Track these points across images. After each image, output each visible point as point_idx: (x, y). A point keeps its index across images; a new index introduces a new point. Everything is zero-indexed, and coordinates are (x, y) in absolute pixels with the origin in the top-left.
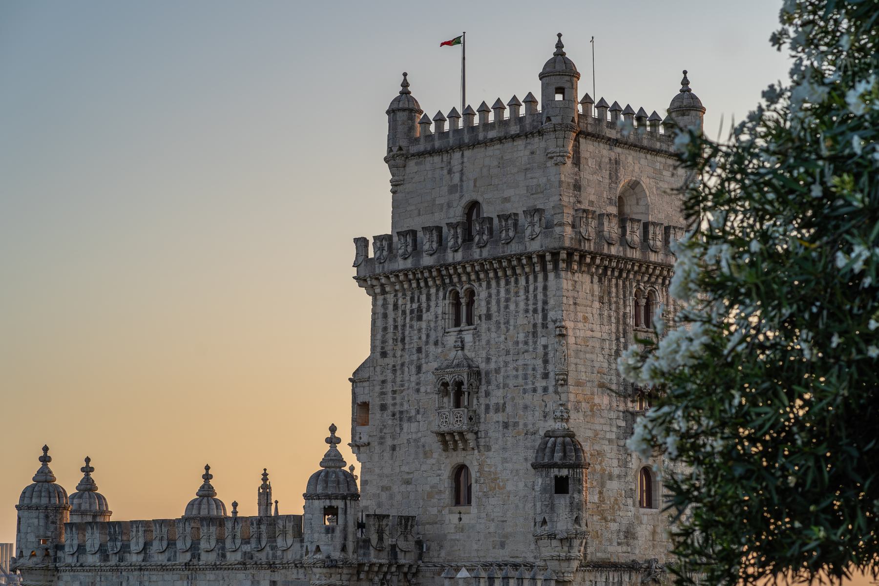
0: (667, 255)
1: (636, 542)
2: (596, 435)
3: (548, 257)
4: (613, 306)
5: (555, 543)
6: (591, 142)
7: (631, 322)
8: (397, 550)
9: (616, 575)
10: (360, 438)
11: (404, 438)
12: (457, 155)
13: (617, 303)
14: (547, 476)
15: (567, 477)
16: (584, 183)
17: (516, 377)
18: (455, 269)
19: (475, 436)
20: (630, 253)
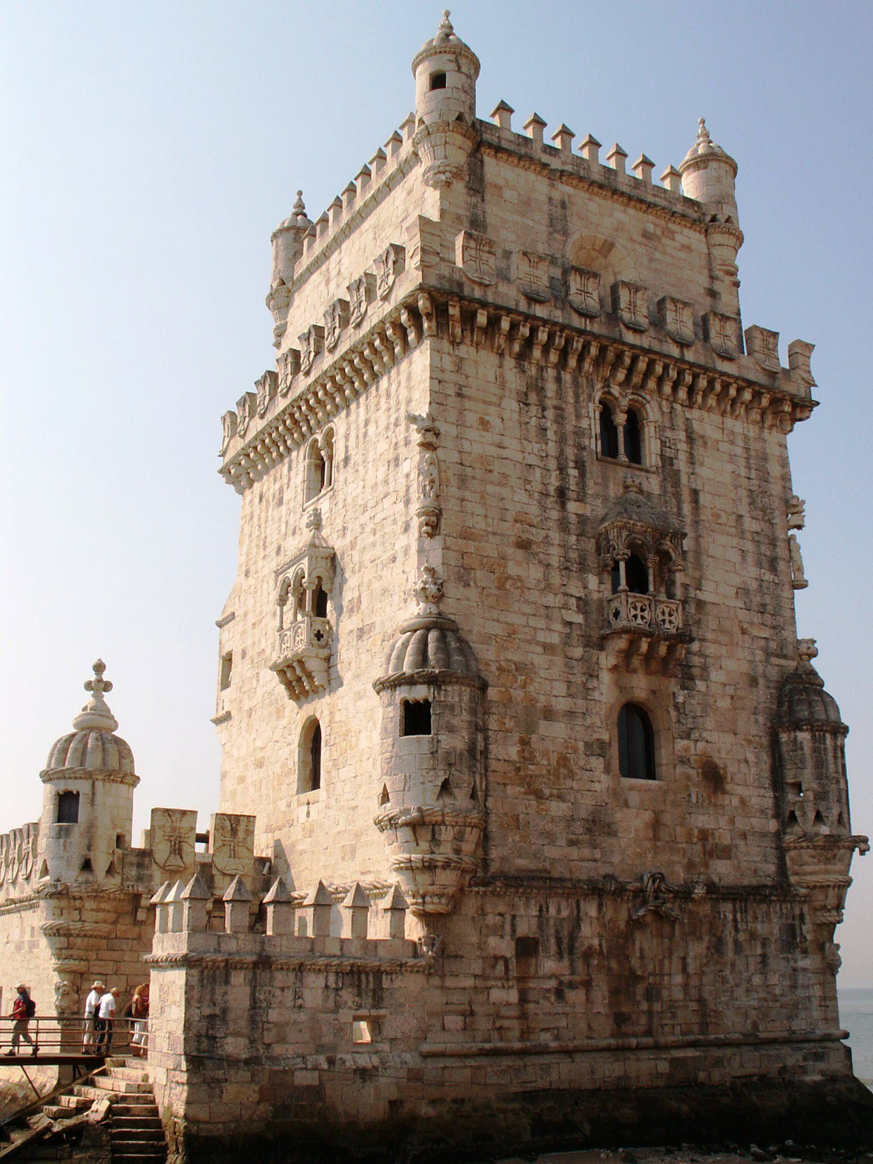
0: (661, 341)
1: (613, 840)
2: (514, 633)
3: (404, 318)
4: (550, 413)
5: (404, 834)
6: (506, 166)
7: (594, 445)
8: (214, 872)
9: (564, 904)
10: (223, 709)
11: (260, 691)
12: (335, 257)
14: (389, 705)
15: (426, 701)
16: (491, 220)
17: (373, 545)
18: (307, 401)
19: (324, 665)
20: (577, 322)
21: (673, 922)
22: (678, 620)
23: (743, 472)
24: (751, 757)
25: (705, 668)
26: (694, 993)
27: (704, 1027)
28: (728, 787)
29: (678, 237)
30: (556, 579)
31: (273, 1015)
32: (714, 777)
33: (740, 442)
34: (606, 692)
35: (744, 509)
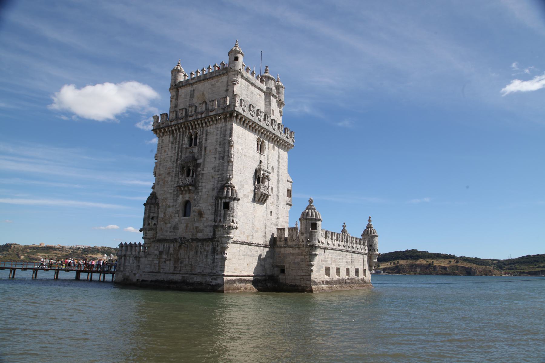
4: (177, 143)
13: (179, 141)
21: (187, 247)
22: (190, 181)
23: (219, 137)
24: (210, 208)
25: (202, 189)
26: (190, 263)
27: (191, 270)
28: (204, 216)
29: (221, 81)
30: (173, 179)
31: (126, 264)
32: (200, 214)
33: (220, 129)
34: (180, 199)
35: (217, 147)
